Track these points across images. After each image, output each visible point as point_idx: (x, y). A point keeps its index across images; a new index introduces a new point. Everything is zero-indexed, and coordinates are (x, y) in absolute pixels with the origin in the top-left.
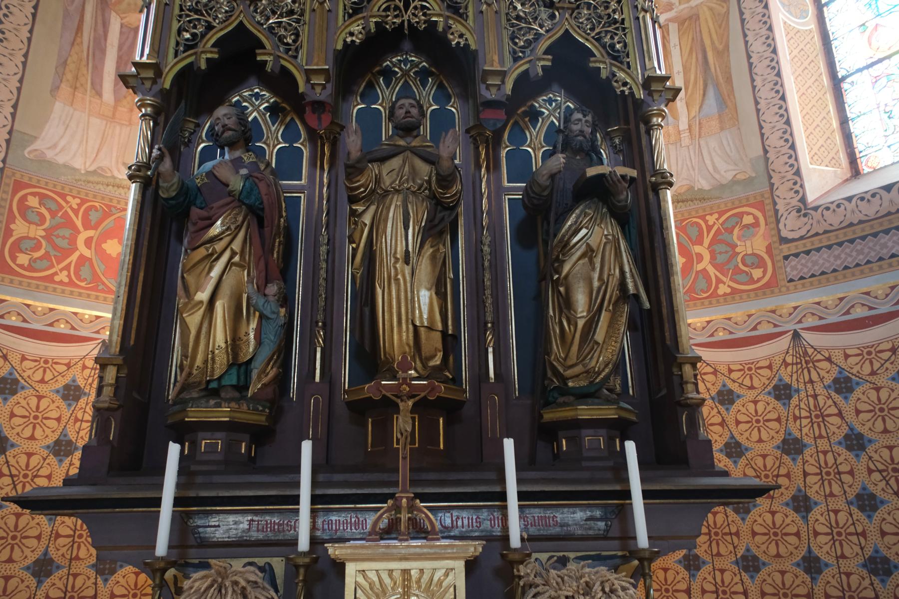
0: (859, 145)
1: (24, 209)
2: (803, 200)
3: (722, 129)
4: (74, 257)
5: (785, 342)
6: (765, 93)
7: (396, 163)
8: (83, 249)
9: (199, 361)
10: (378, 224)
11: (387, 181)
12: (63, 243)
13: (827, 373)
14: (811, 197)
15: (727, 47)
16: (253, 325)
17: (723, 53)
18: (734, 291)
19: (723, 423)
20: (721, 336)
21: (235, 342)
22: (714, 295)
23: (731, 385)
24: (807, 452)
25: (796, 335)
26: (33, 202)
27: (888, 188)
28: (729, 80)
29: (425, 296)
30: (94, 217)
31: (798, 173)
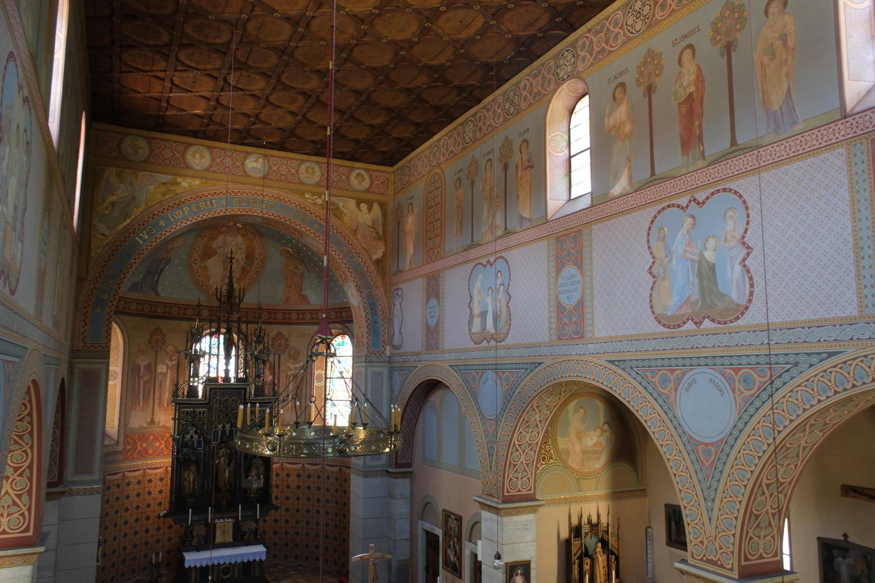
1: (128, 442)
4: (137, 450)
5: (301, 465)
7: (223, 450)
8: (139, 448)
9: (187, 489)
10: (219, 463)
11: (221, 454)
12: (135, 448)
13: (307, 473)
16: (196, 483)
19: (287, 481)
21: (194, 486)
25: (303, 464)
26: (129, 440)
29: (227, 475)
30: (140, 438)
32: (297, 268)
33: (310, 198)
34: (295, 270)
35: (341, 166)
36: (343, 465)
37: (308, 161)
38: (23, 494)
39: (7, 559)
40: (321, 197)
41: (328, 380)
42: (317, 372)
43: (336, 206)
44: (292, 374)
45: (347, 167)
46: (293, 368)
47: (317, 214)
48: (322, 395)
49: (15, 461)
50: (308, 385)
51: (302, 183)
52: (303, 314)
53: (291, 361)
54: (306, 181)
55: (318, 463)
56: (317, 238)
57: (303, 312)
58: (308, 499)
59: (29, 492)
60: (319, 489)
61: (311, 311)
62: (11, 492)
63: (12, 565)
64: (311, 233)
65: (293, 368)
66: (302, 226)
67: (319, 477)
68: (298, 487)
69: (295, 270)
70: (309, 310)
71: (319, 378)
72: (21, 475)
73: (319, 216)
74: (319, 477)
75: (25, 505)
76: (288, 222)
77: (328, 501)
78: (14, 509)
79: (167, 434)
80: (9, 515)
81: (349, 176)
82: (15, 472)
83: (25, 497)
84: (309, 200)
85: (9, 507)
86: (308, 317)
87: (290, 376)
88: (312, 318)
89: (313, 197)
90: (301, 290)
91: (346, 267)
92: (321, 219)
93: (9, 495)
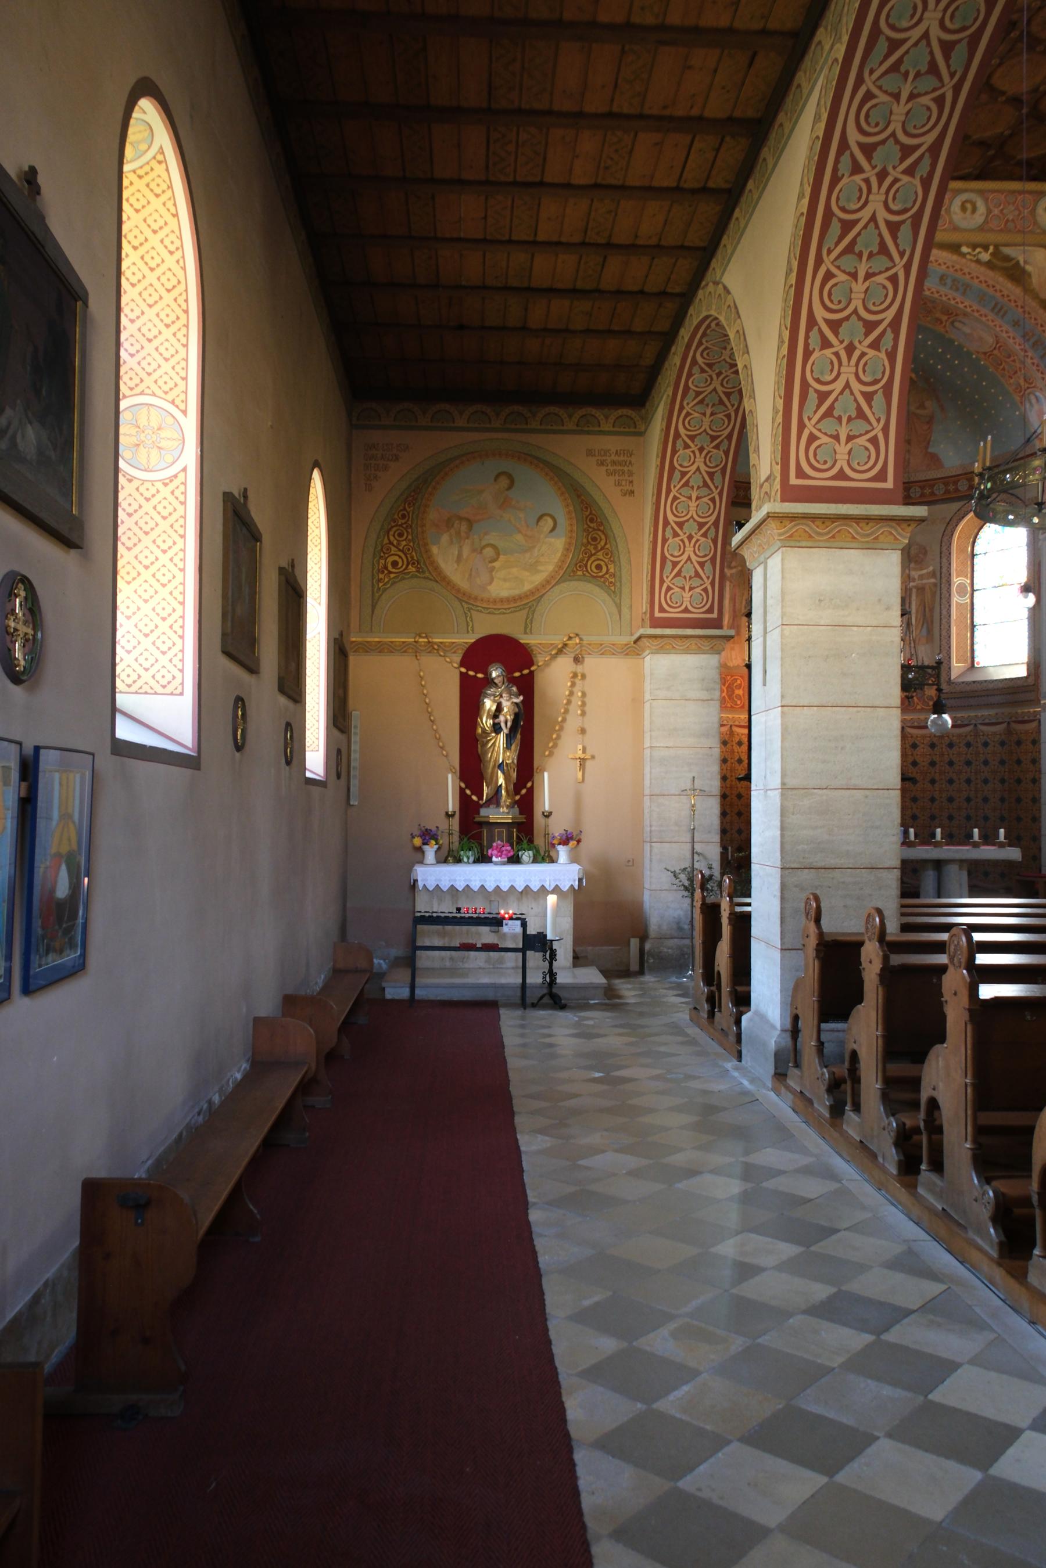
0: (976, 654)
2: (950, 678)
3: (927, 643)
6: (944, 633)
14: (952, 678)
15: (933, 608)
17: (932, 610)
18: (922, 709)
19: (912, 755)
20: (916, 724)
22: (915, 709)
23: (917, 742)
24: (937, 766)
27: (974, 682)
28: (932, 622)
31: (950, 668)
32: (922, 406)
33: (969, 253)
34: (919, 411)
35: (1020, 192)
36: (1014, 719)
37: (966, 191)
38: (706, 561)
39: (694, 641)
40: (988, 249)
41: (975, 593)
42: (957, 581)
43: (1014, 262)
44: (914, 587)
45: (1030, 192)
46: (916, 577)
47: (982, 278)
48: (966, 617)
49: (701, 514)
50: (944, 601)
51: (956, 229)
52: (933, 486)
53: (912, 565)
54: (963, 224)
55: (965, 723)
56: (984, 319)
57: (931, 483)
58: (951, 781)
59: (713, 560)
60: (968, 763)
61: (945, 480)
62: (694, 558)
63: (699, 651)
64: (973, 311)
65: (916, 577)
66: (958, 300)
67: (968, 745)
68: (933, 764)
69: (919, 411)
70: (940, 479)
71: (962, 590)
72: (705, 535)
73: (986, 282)
74: (968, 745)
75: (708, 578)
76: (936, 295)
77: (986, 781)
78: (696, 582)
79: (729, 678)
80: (691, 589)
81: (1034, 210)
82: (700, 529)
83: (708, 566)
84: (968, 257)
85: (691, 578)
86: (939, 490)
87: (911, 590)
88: (947, 492)
89: (974, 249)
90: (927, 447)
91: (1033, 364)
92: (988, 286)
93: (692, 563)
